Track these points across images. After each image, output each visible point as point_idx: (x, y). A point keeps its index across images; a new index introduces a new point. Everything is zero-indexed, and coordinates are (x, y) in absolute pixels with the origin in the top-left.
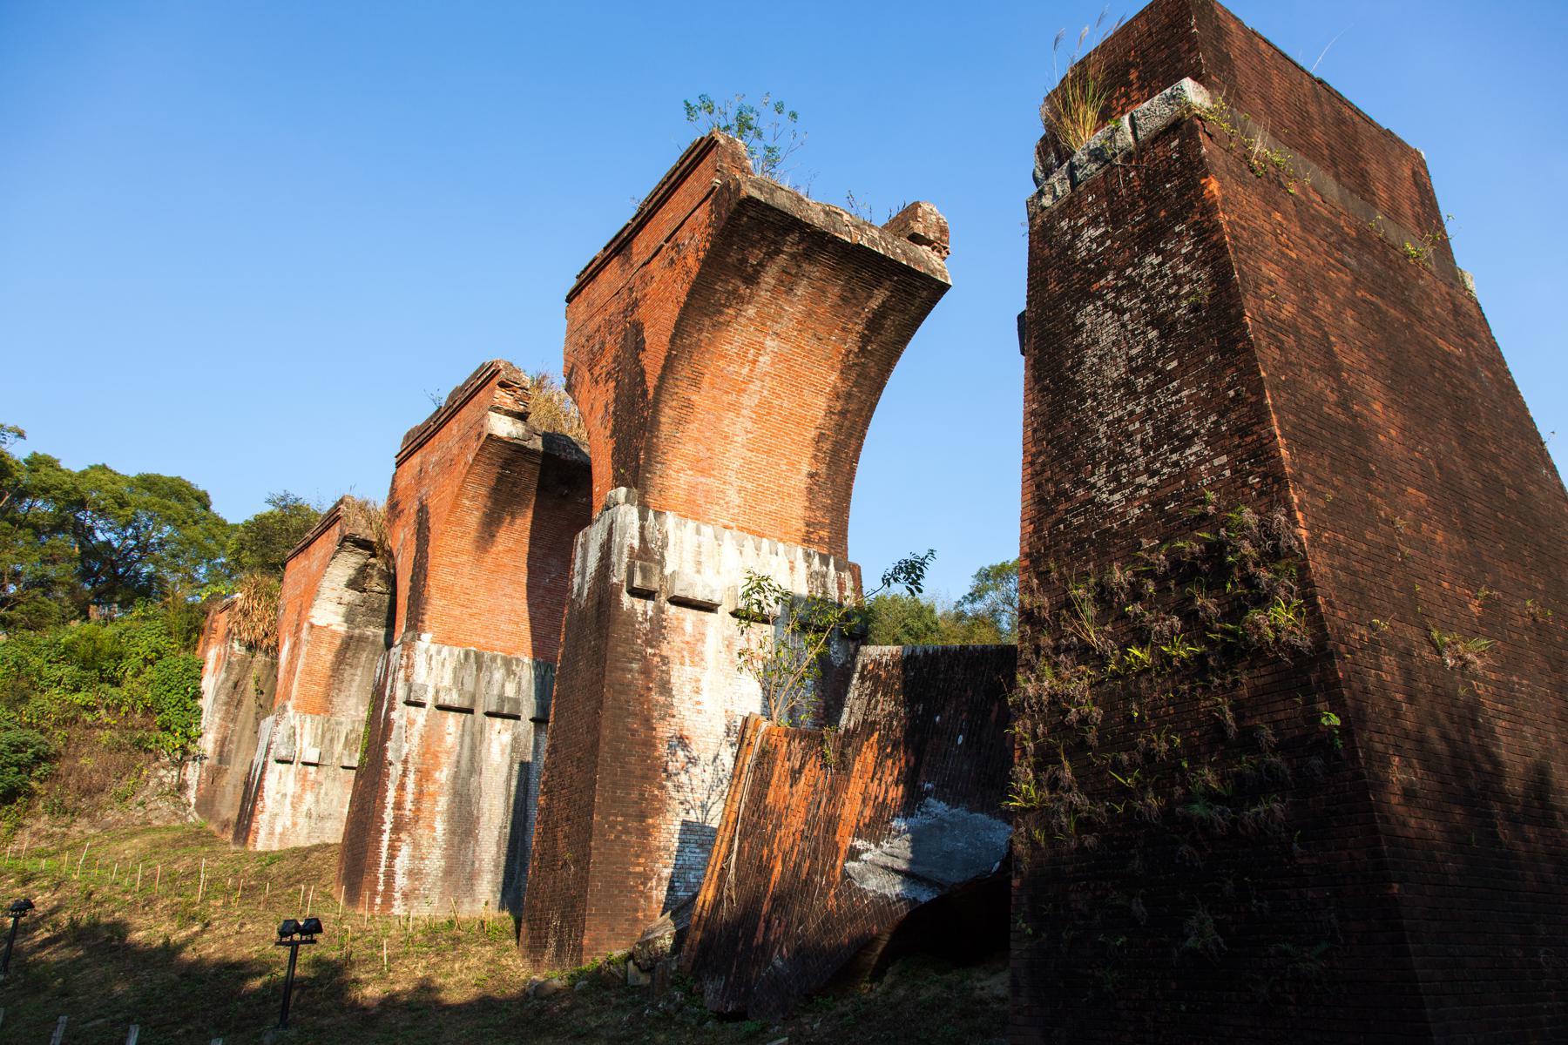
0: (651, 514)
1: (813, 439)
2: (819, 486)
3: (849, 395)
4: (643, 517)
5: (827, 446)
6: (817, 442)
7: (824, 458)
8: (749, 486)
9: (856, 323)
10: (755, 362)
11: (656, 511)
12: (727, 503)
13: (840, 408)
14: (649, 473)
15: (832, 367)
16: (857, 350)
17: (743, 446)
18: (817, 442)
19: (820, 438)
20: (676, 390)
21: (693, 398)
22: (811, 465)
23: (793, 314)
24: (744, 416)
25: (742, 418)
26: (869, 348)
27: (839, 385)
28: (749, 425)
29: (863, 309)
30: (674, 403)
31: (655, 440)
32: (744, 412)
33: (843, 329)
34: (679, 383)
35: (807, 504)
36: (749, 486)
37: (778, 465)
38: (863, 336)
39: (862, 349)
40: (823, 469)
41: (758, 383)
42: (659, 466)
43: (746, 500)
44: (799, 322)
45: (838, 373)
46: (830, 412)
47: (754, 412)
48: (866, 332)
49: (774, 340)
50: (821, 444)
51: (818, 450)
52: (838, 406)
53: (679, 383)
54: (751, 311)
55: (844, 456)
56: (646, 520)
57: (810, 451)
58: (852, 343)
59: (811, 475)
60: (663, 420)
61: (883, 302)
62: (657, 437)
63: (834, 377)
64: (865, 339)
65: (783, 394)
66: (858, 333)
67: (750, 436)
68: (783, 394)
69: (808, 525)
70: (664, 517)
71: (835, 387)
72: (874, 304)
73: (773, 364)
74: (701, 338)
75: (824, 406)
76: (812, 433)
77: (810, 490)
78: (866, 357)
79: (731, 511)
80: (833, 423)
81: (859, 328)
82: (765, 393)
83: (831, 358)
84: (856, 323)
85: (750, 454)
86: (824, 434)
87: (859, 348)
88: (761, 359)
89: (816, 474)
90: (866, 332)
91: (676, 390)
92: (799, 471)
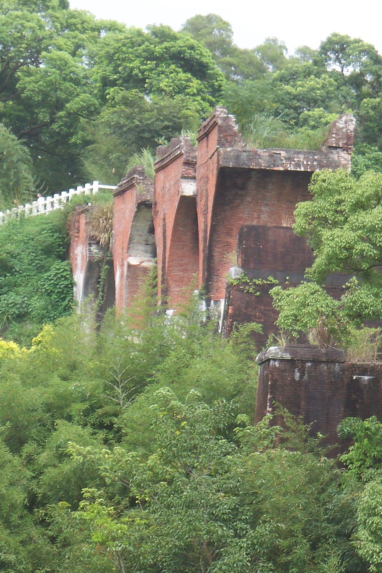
0: (212, 302)
4: (208, 305)
10: (259, 218)
11: (215, 300)
14: (211, 281)
20: (219, 239)
21: (229, 240)
30: (220, 245)
31: (212, 265)
34: (220, 236)
42: (215, 277)
53: (220, 236)
54: (249, 199)
56: (210, 306)
60: (215, 254)
62: (213, 263)
70: (219, 302)
74: (226, 214)
91: (219, 239)
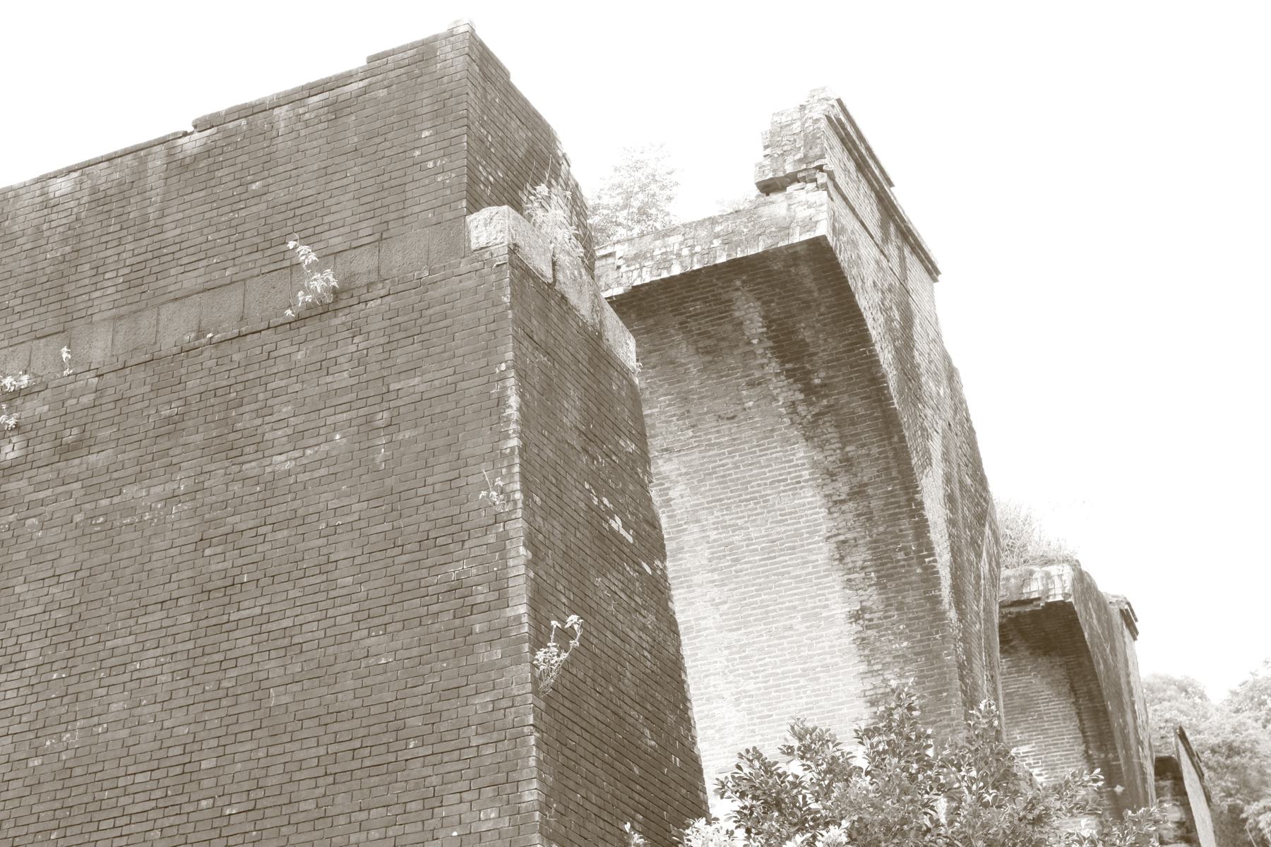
1: (832, 559)
2: (877, 626)
3: (848, 463)
5: (861, 556)
6: (841, 559)
7: (867, 577)
8: (750, 686)
9: (762, 366)
12: (718, 731)
13: (846, 489)
15: (786, 441)
16: (802, 396)
17: (720, 629)
18: (841, 559)
19: (843, 549)
22: (848, 600)
23: (662, 413)
24: (700, 586)
25: (699, 590)
26: (817, 381)
27: (819, 457)
28: (714, 593)
29: (749, 343)
32: (697, 579)
33: (751, 384)
35: (863, 667)
36: (750, 686)
37: (791, 628)
38: (790, 374)
39: (809, 390)
40: (872, 597)
41: (695, 528)
43: (750, 712)
44: (681, 417)
45: (802, 442)
46: (835, 504)
47: (714, 571)
48: (788, 366)
49: (670, 460)
50: (848, 559)
51: (851, 571)
52: (842, 487)
55: (901, 556)
57: (836, 579)
58: (784, 392)
59: (856, 617)
61: (764, 317)
63: (801, 452)
64: (799, 376)
65: (740, 522)
66: (777, 375)
67: (724, 608)
68: (740, 522)
69: (873, 703)
71: (815, 464)
72: (755, 325)
73: (694, 491)
75: (819, 500)
76: (823, 552)
77: (862, 642)
78: (826, 396)
79: (730, 740)
80: (850, 516)
81: (773, 367)
82: (713, 535)
83: (772, 430)
84: (762, 366)
85: (735, 635)
86: (844, 542)
87: (801, 391)
88: (672, 494)
89: (863, 609)
90: (788, 366)
92: (830, 620)
